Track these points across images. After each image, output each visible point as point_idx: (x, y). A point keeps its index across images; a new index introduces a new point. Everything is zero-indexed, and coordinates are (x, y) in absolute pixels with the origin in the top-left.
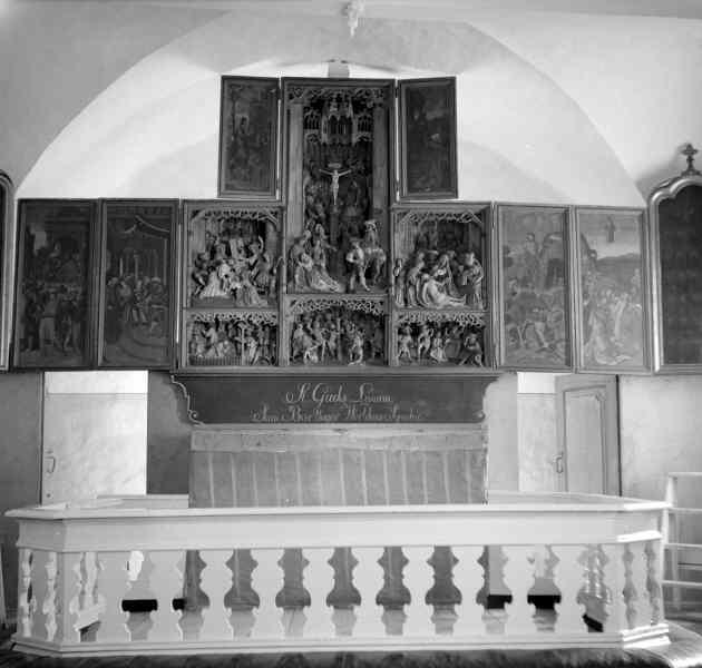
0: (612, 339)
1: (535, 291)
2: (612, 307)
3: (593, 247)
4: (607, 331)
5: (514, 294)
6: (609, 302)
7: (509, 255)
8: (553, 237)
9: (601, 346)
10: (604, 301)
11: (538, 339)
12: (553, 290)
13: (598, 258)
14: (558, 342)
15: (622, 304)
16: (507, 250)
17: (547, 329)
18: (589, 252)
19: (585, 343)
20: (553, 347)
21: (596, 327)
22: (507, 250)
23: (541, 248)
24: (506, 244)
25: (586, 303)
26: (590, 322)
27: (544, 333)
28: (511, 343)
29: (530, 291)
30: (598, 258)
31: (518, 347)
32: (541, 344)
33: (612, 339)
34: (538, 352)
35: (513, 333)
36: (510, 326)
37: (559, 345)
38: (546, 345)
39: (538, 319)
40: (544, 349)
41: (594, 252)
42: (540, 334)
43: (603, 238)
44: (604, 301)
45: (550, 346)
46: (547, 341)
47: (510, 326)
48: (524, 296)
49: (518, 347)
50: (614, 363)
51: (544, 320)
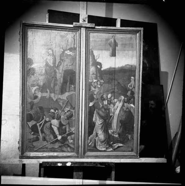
1: (52, 95)
3: (98, 60)
5: (36, 97)
6: (110, 102)
8: (68, 52)
9: (101, 136)
10: (106, 103)
13: (102, 69)
17: (61, 125)
26: (94, 120)
27: (59, 129)
30: (102, 69)
32: (55, 137)
33: (110, 131)
34: (53, 143)
37: (69, 137)
38: (59, 137)
40: (57, 141)
41: (100, 64)
42: (55, 129)
43: (107, 53)
44: (106, 103)
45: (62, 138)
46: (60, 134)
49: (37, 139)
51: (59, 118)
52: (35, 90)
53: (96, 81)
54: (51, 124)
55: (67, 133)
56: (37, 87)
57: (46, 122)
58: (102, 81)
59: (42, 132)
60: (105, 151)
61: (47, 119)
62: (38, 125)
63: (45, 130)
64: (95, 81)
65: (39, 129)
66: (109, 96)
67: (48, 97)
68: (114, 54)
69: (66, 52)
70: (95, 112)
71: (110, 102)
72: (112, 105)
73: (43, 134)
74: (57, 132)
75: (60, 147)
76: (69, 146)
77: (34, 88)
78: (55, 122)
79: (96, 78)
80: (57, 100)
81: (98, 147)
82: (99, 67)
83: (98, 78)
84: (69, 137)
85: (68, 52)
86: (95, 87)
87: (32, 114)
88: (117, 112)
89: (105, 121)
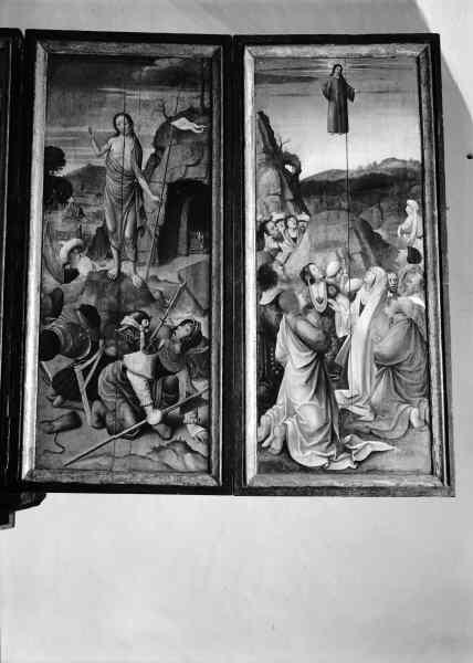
0: (340, 395)
1: (127, 268)
2: (340, 306)
3: (288, 148)
4: (328, 372)
6: (334, 291)
7: (63, 173)
8: (183, 124)
9: (312, 416)
10: (318, 291)
11: (134, 401)
12: (182, 263)
13: (302, 177)
14: (185, 408)
15: (371, 299)
16: (54, 158)
17: (159, 371)
18: (276, 156)
19: (261, 410)
20: (174, 424)
21: (295, 362)
22: (54, 158)
23: (148, 151)
24: (53, 142)
25: (267, 297)
26: (278, 352)
27: (150, 384)
28: (57, 412)
29: (111, 267)
30: (302, 177)
31: (76, 422)
32: (140, 414)
33: (340, 395)
35: (63, 386)
36: (60, 363)
37: (188, 417)
38: (154, 417)
39: (134, 348)
41: (292, 159)
42: (139, 386)
43: (318, 115)
44: (318, 291)
45: (165, 420)
46: (155, 406)
47: (60, 363)
48: (97, 283)
49: (76, 422)
50: (345, 464)
51: (152, 347)
52: (72, 251)
53: (281, 216)
54: (125, 369)
55: (182, 400)
56: (74, 242)
57: (106, 360)
58: (305, 217)
59: (93, 395)
60: (323, 470)
61: (111, 351)
62: (78, 369)
63: (101, 390)
64: (277, 216)
65: (83, 386)
66: (332, 267)
67: (113, 272)
68: (340, 125)
69: (176, 123)
70: (282, 325)
71: (334, 291)
72: (342, 300)
73: (97, 404)
74: (145, 398)
75: (157, 450)
76: (188, 449)
77: (68, 245)
78: (138, 364)
79: (282, 208)
80: (144, 285)
81: (296, 454)
82: (289, 167)
83: (290, 206)
84: (188, 417)
85: (183, 124)
86: (279, 239)
87: (59, 332)
88: (363, 323)
89: (320, 356)
